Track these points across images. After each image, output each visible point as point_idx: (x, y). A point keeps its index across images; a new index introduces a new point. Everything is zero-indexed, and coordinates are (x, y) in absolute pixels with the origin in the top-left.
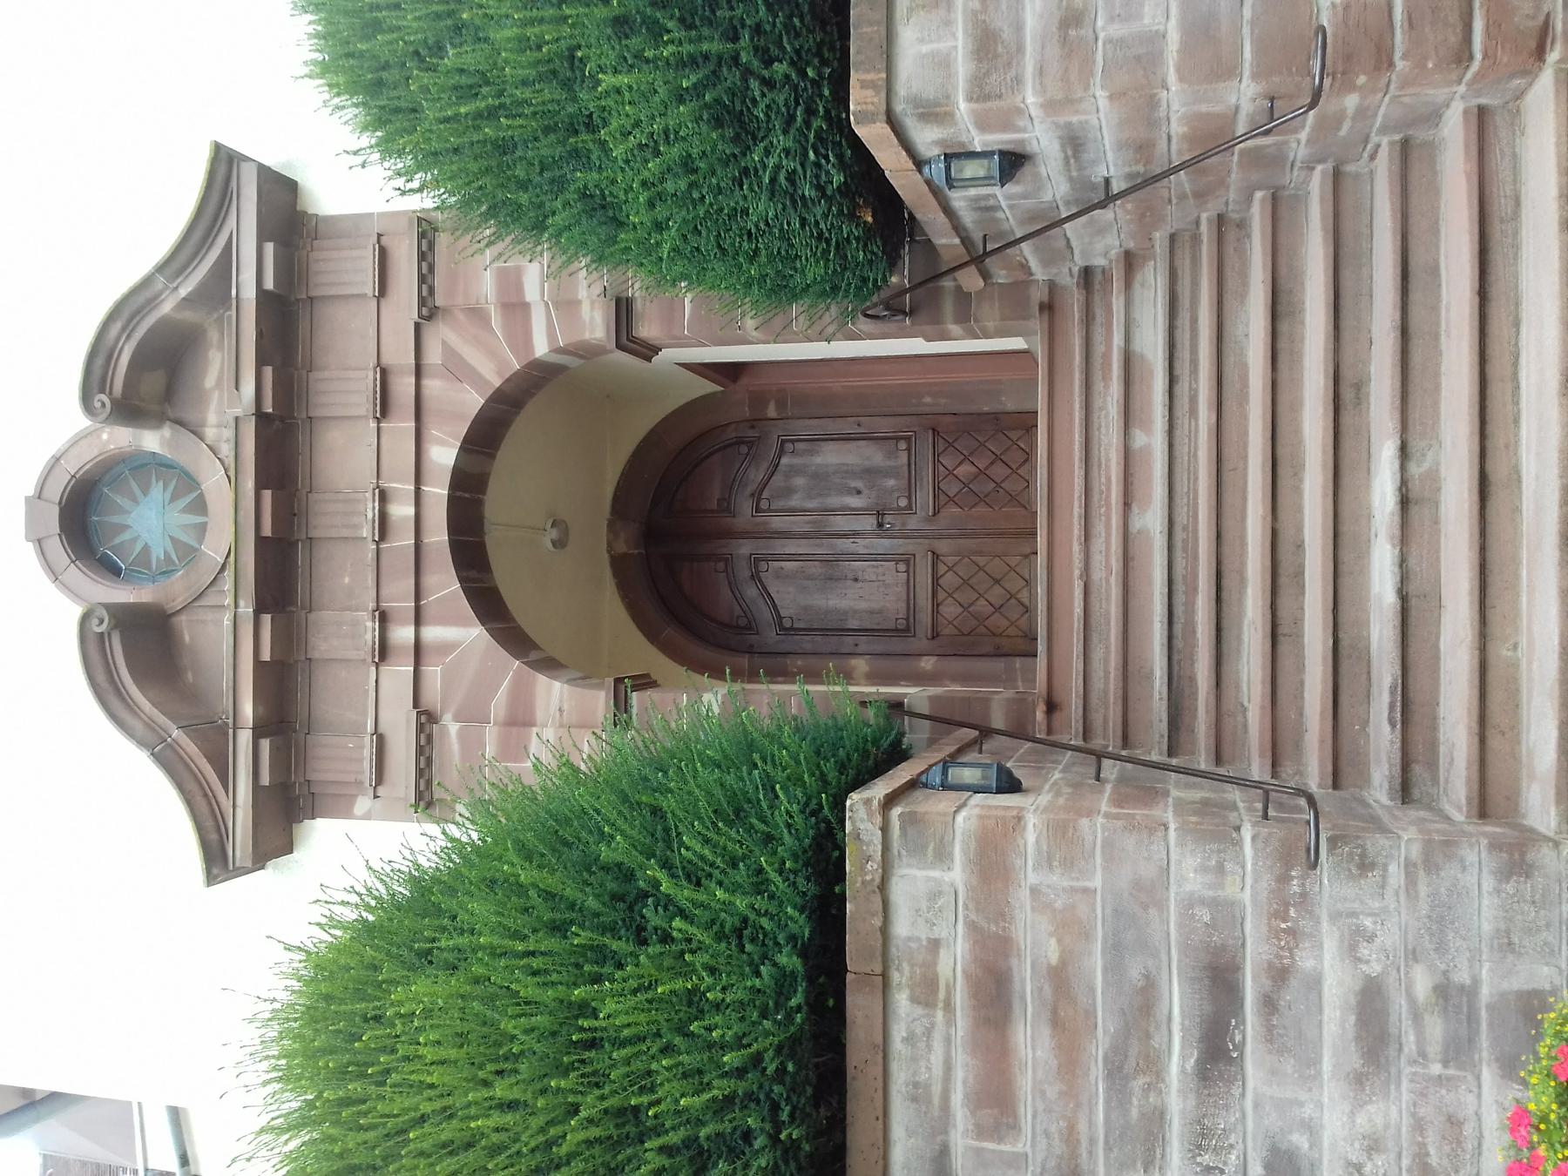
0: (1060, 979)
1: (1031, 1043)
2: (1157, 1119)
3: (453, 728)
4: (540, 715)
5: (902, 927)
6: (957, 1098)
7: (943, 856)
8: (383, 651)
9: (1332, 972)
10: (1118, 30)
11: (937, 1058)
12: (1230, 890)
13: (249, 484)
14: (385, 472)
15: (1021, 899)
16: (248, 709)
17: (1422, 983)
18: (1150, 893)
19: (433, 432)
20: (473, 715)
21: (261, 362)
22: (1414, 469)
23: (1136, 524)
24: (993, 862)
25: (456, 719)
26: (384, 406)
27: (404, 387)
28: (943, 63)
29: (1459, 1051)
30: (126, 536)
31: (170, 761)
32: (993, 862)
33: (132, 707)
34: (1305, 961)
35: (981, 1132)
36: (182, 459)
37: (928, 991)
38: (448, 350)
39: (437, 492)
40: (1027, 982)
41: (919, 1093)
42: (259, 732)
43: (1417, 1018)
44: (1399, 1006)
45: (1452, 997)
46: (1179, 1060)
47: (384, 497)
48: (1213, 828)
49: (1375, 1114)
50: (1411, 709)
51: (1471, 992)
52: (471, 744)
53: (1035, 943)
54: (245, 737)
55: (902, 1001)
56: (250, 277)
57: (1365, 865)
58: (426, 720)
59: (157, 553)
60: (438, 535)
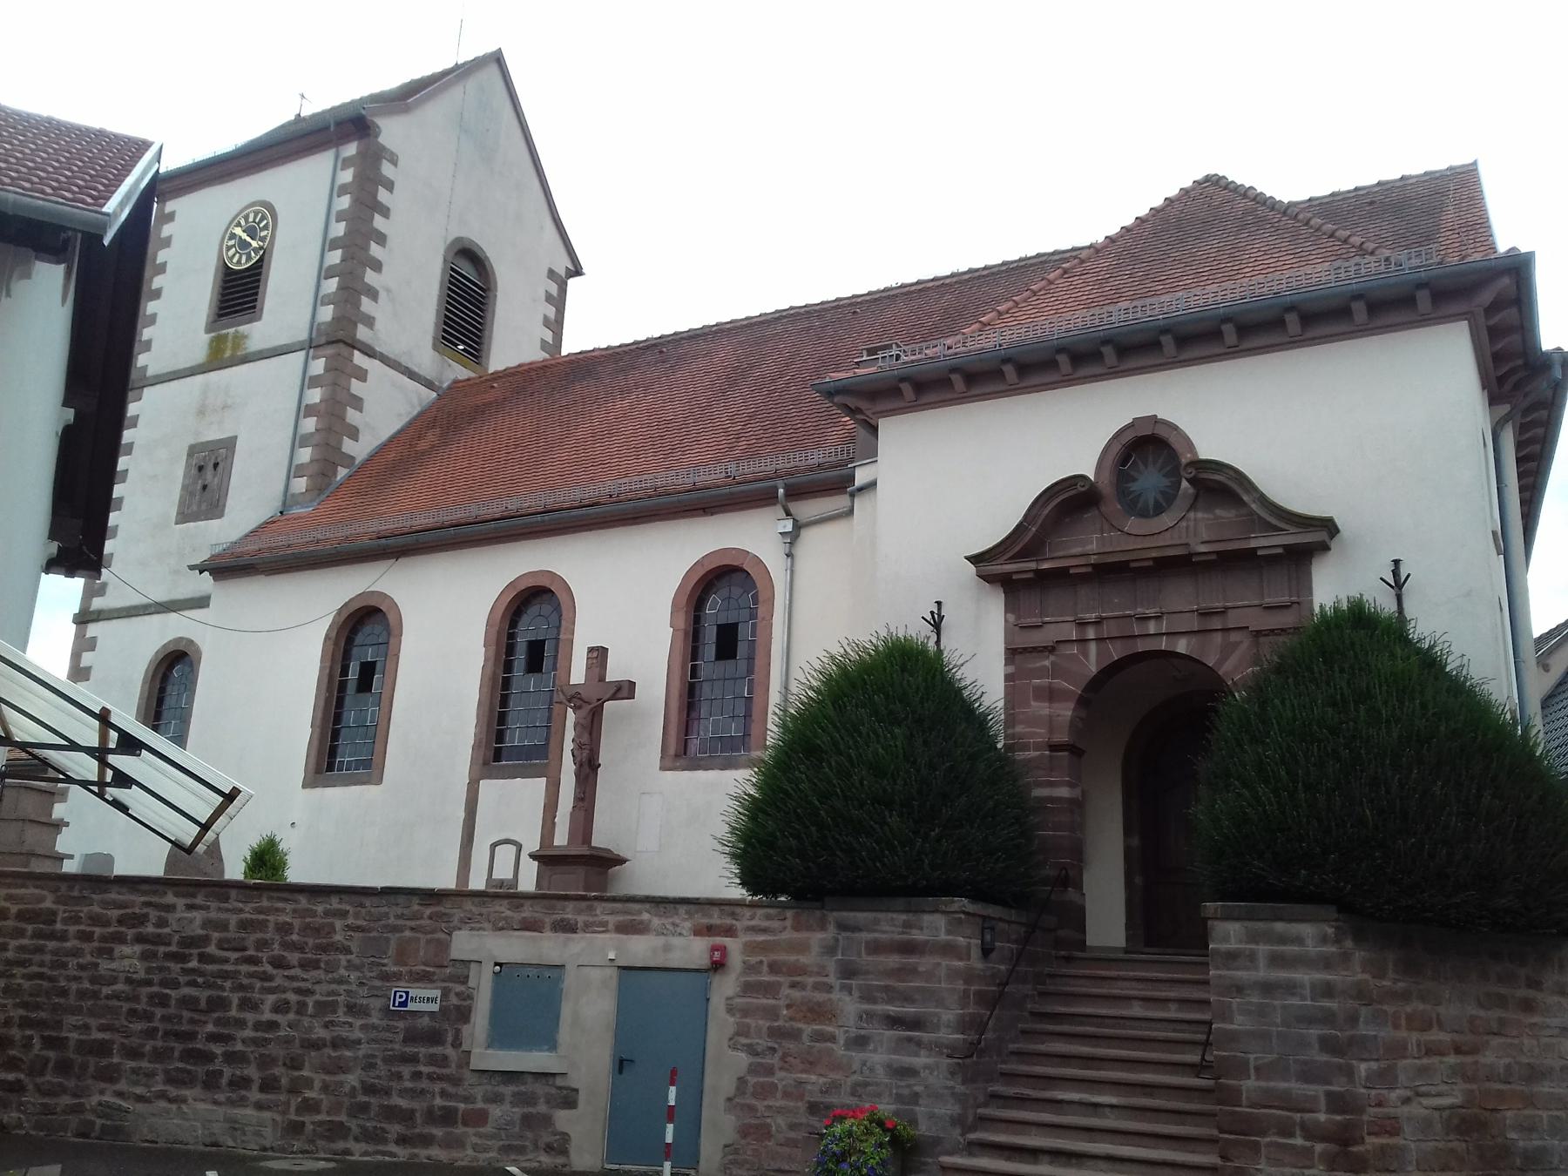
0: (912, 971)
1: (893, 960)
2: (874, 1001)
3: (1047, 663)
4: (1055, 705)
5: (927, 918)
6: (876, 935)
7: (949, 932)
8: (1082, 624)
9: (921, 1060)
10: (1234, 1006)
11: (887, 928)
12: (943, 1030)
13: (1154, 555)
14: (1171, 622)
15: (937, 959)
16: (1045, 566)
17: (918, 1089)
18: (940, 1003)
19: (1194, 639)
20: (1056, 671)
21: (1217, 553)
22: (1107, 1110)
23: (1135, 1003)
24: (948, 949)
25: (1053, 663)
26: (1205, 614)
27: (1216, 623)
28: (1226, 939)
29: (899, 1098)
30: (1142, 467)
31: (1020, 529)
32: (948, 949)
33: (1044, 505)
34: (923, 1052)
35: (867, 943)
36: (1178, 501)
37: (907, 926)
38: (1237, 644)
39: (1163, 644)
40: (913, 960)
41: (877, 922)
42: (1037, 571)
43: (909, 1086)
44: (912, 1081)
45: (915, 1098)
46: (892, 1009)
47: (1158, 618)
48: (963, 1025)
49: (880, 1071)
50: (1022, 1101)
51: (917, 1104)
52: (1042, 672)
53: (925, 963)
54: (1033, 565)
55: (904, 917)
56: (1262, 542)
57: (952, 1074)
58: (1051, 650)
59: (1135, 487)
60: (1142, 646)
